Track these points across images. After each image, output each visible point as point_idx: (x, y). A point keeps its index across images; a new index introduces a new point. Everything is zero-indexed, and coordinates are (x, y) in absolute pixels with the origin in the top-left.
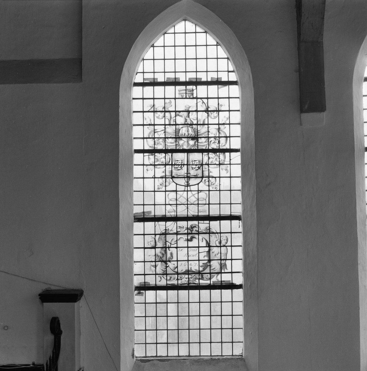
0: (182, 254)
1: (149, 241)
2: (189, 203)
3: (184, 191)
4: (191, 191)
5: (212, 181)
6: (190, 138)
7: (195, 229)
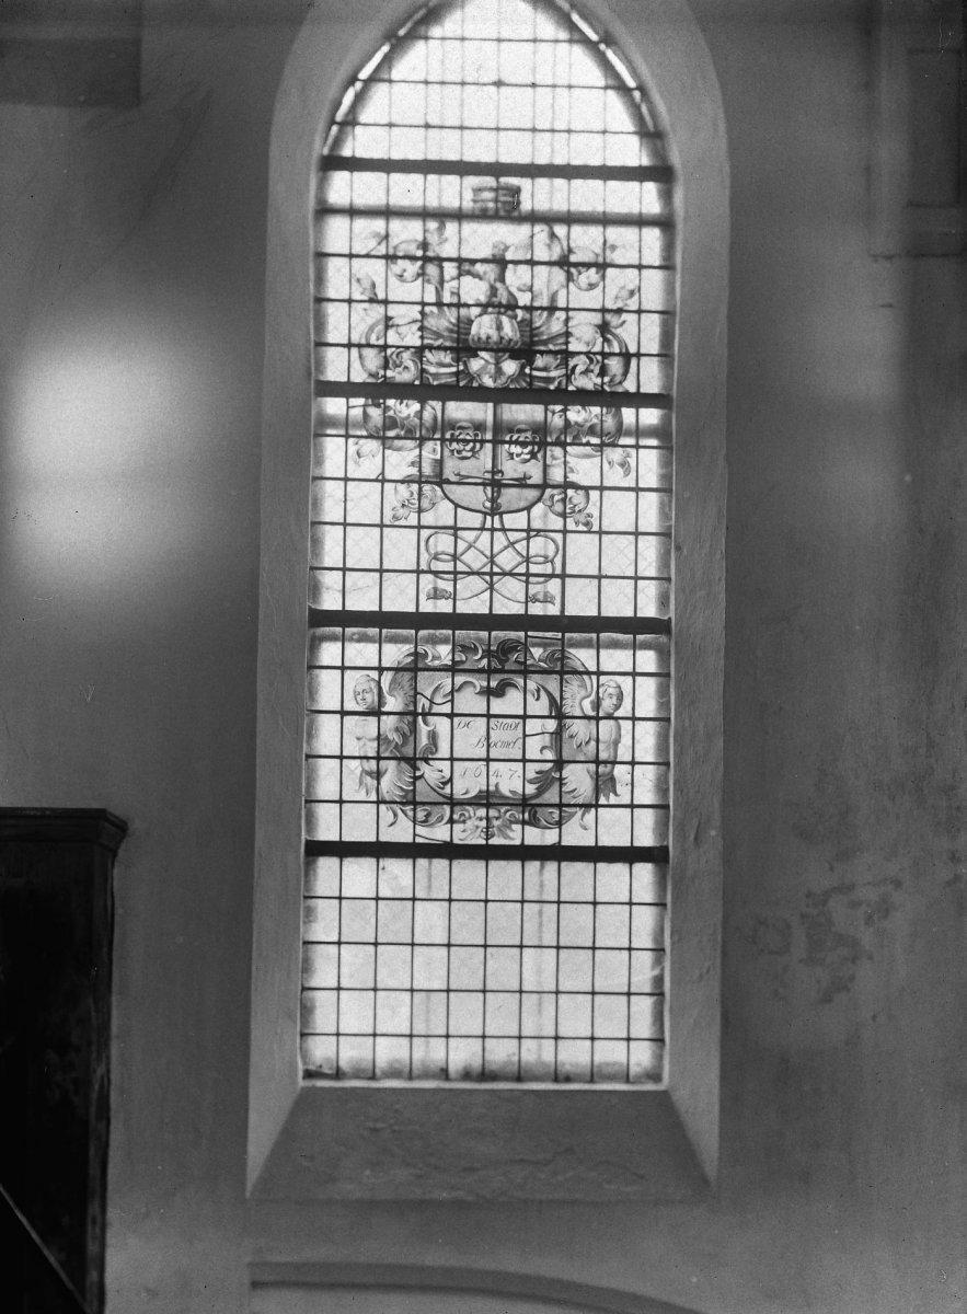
1: (359, 689)
2: (496, 570)
3: (482, 529)
4: (503, 530)
5: (575, 501)
6: (504, 350)
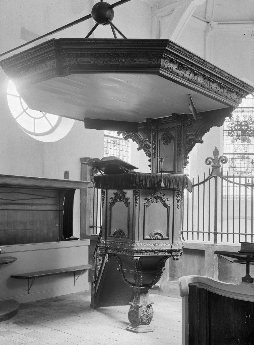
0: (239, 165)
7: (243, 157)
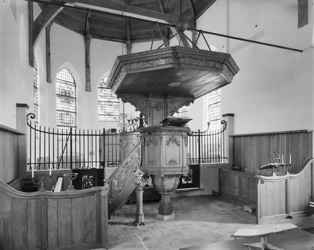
0: (65, 119)
